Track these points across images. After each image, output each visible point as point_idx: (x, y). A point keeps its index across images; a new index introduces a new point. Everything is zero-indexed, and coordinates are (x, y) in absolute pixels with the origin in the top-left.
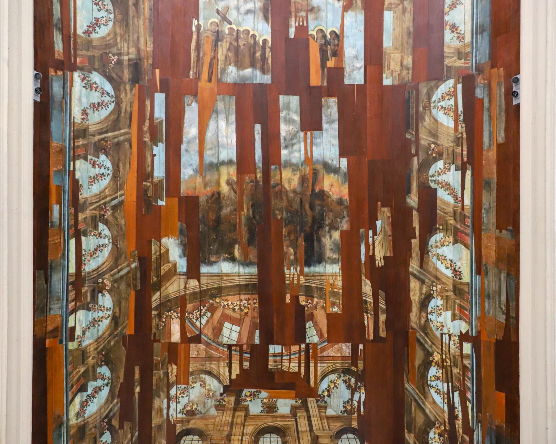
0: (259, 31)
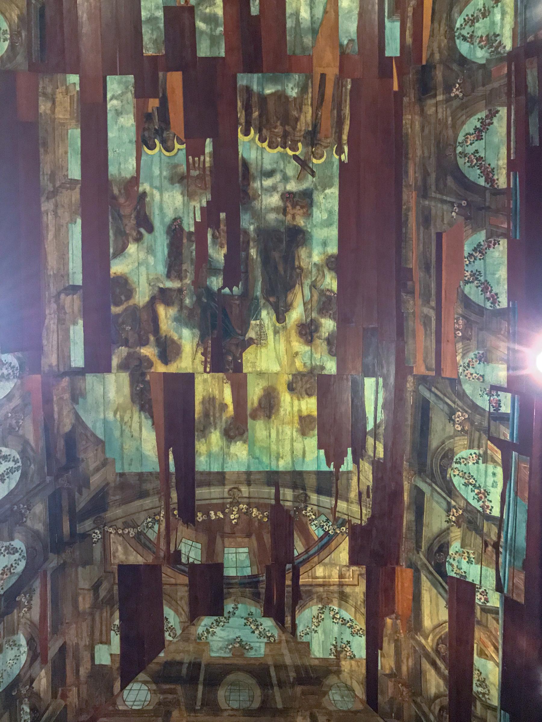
0: (255, 147)
